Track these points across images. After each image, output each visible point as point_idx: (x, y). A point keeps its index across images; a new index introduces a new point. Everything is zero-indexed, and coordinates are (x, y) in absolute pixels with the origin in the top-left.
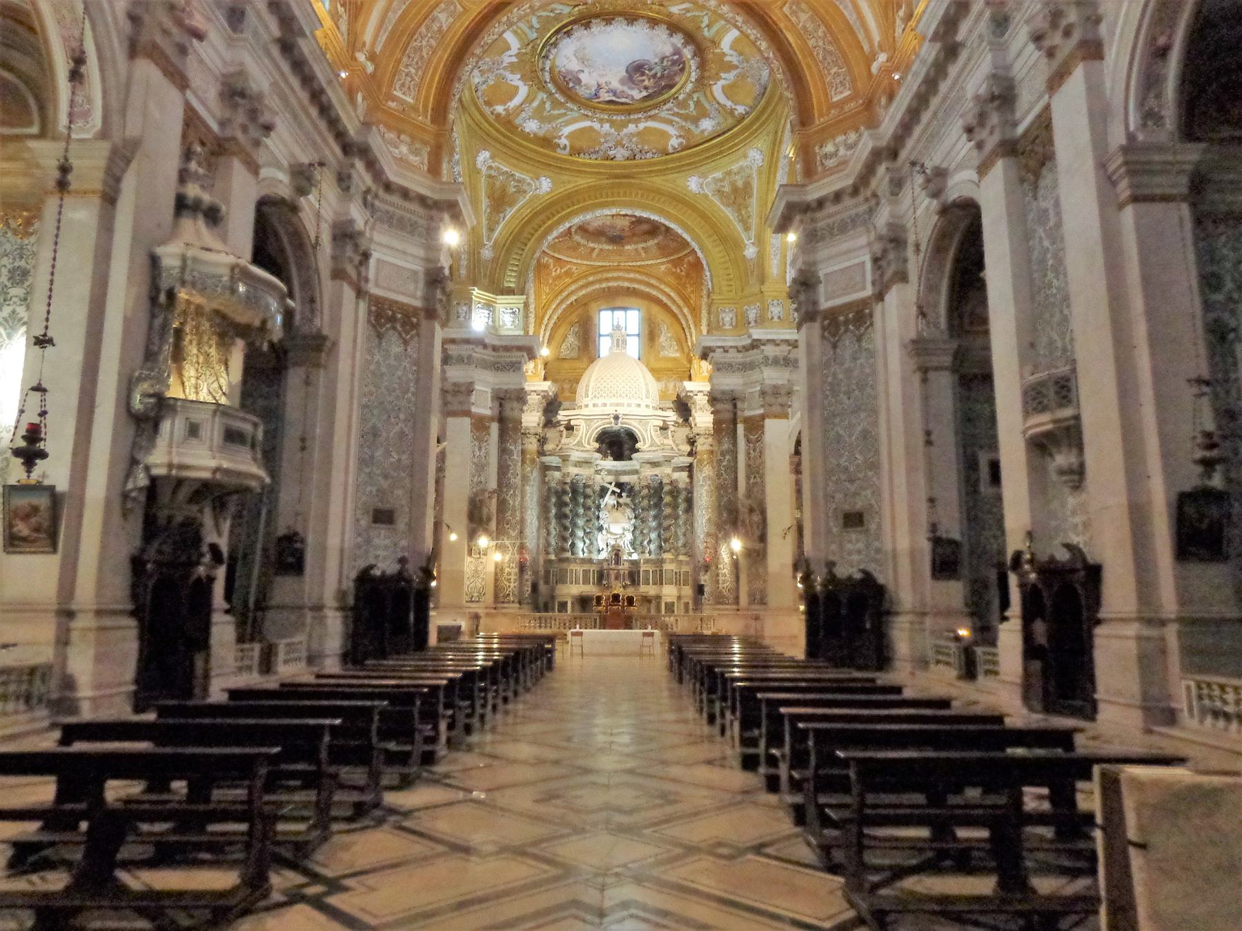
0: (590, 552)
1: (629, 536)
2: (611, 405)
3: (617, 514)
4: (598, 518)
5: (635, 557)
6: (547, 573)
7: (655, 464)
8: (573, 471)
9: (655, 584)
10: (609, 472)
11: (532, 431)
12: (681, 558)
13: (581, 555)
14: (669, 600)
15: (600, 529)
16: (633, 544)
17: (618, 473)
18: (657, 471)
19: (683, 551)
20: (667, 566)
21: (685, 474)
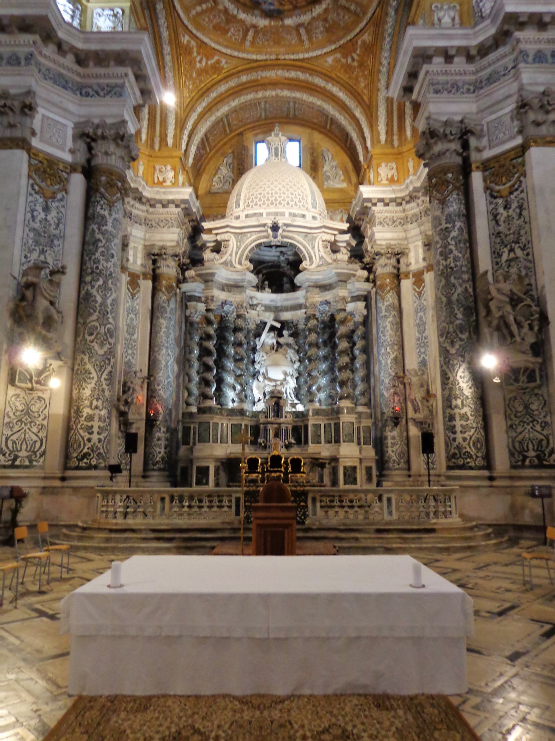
0: (241, 401)
1: (292, 383)
2: (268, 214)
3: (278, 356)
4: (253, 362)
5: (300, 408)
6: (186, 430)
7: (325, 287)
8: (220, 295)
9: (329, 442)
10: (268, 308)
11: (170, 252)
12: (360, 409)
13: (230, 405)
14: (349, 464)
15: (255, 375)
16: (297, 393)
17: (276, 310)
18: (328, 296)
19: (363, 400)
20: (346, 418)
21: (361, 305)
